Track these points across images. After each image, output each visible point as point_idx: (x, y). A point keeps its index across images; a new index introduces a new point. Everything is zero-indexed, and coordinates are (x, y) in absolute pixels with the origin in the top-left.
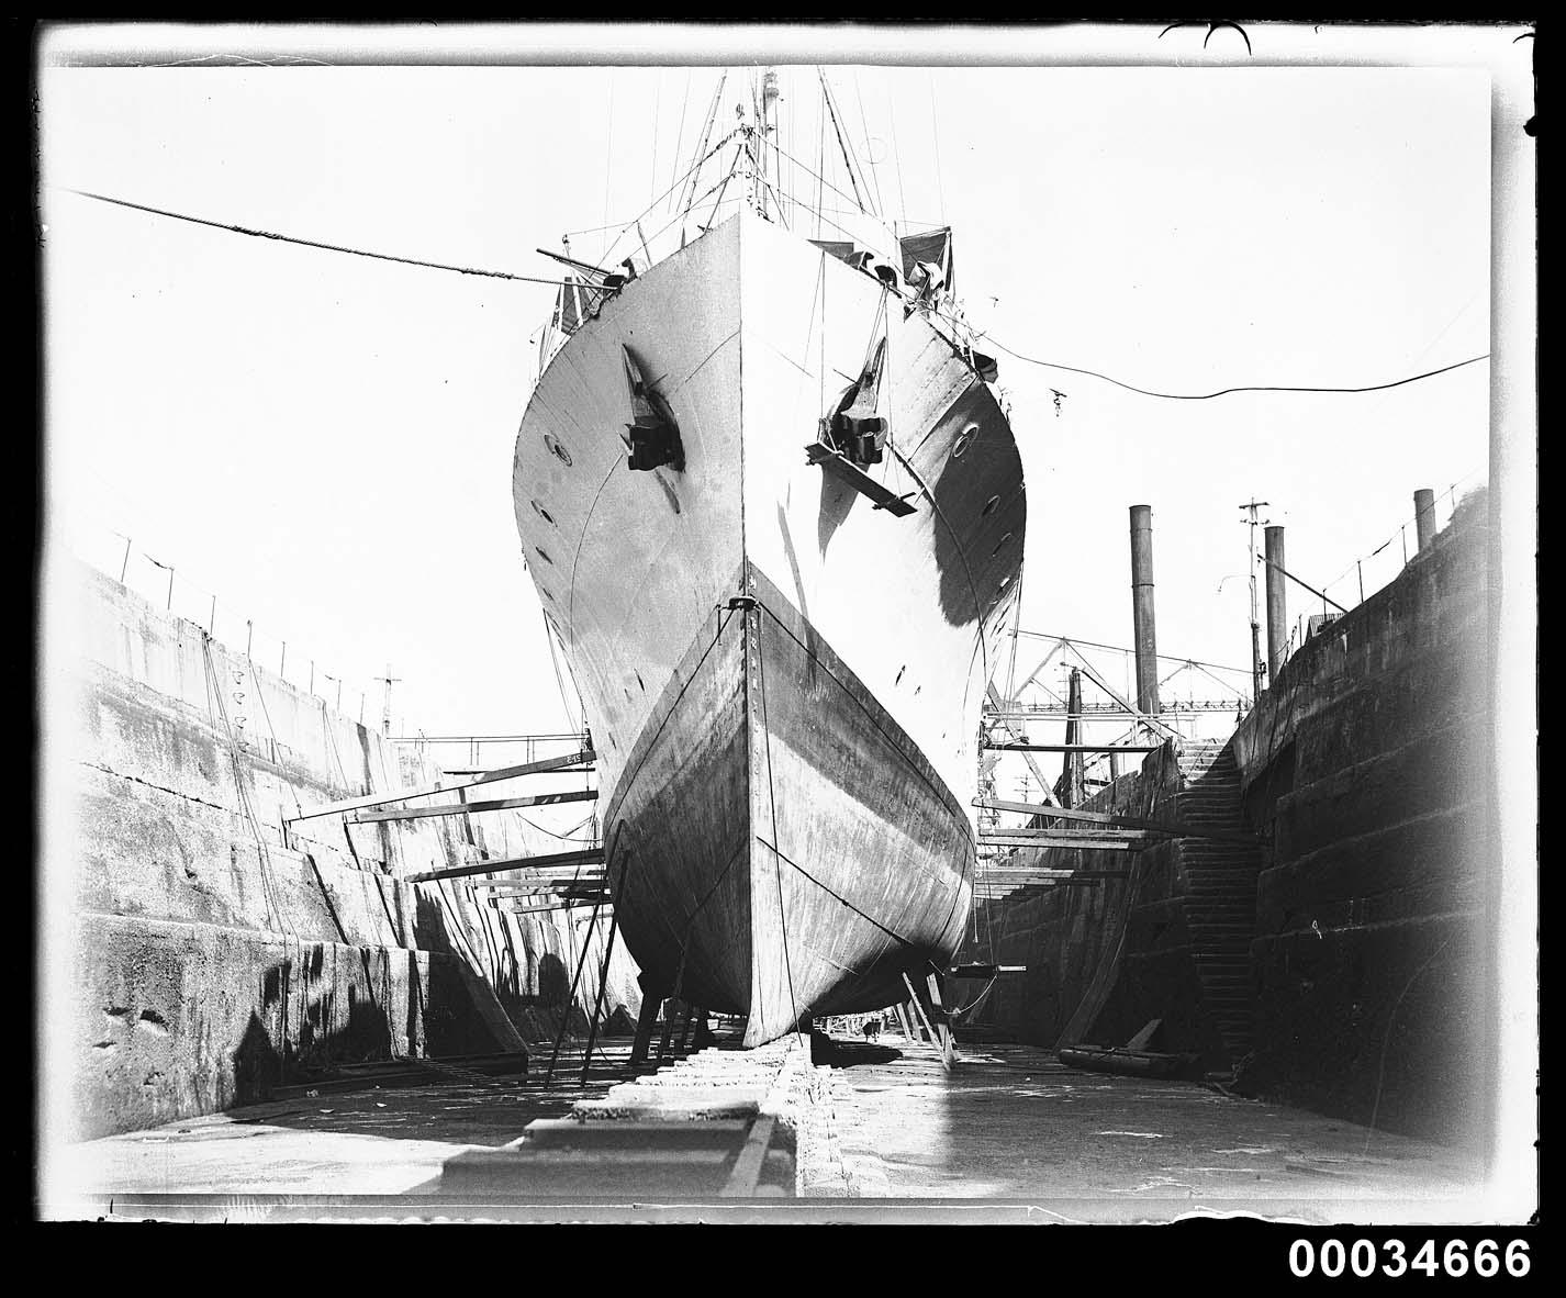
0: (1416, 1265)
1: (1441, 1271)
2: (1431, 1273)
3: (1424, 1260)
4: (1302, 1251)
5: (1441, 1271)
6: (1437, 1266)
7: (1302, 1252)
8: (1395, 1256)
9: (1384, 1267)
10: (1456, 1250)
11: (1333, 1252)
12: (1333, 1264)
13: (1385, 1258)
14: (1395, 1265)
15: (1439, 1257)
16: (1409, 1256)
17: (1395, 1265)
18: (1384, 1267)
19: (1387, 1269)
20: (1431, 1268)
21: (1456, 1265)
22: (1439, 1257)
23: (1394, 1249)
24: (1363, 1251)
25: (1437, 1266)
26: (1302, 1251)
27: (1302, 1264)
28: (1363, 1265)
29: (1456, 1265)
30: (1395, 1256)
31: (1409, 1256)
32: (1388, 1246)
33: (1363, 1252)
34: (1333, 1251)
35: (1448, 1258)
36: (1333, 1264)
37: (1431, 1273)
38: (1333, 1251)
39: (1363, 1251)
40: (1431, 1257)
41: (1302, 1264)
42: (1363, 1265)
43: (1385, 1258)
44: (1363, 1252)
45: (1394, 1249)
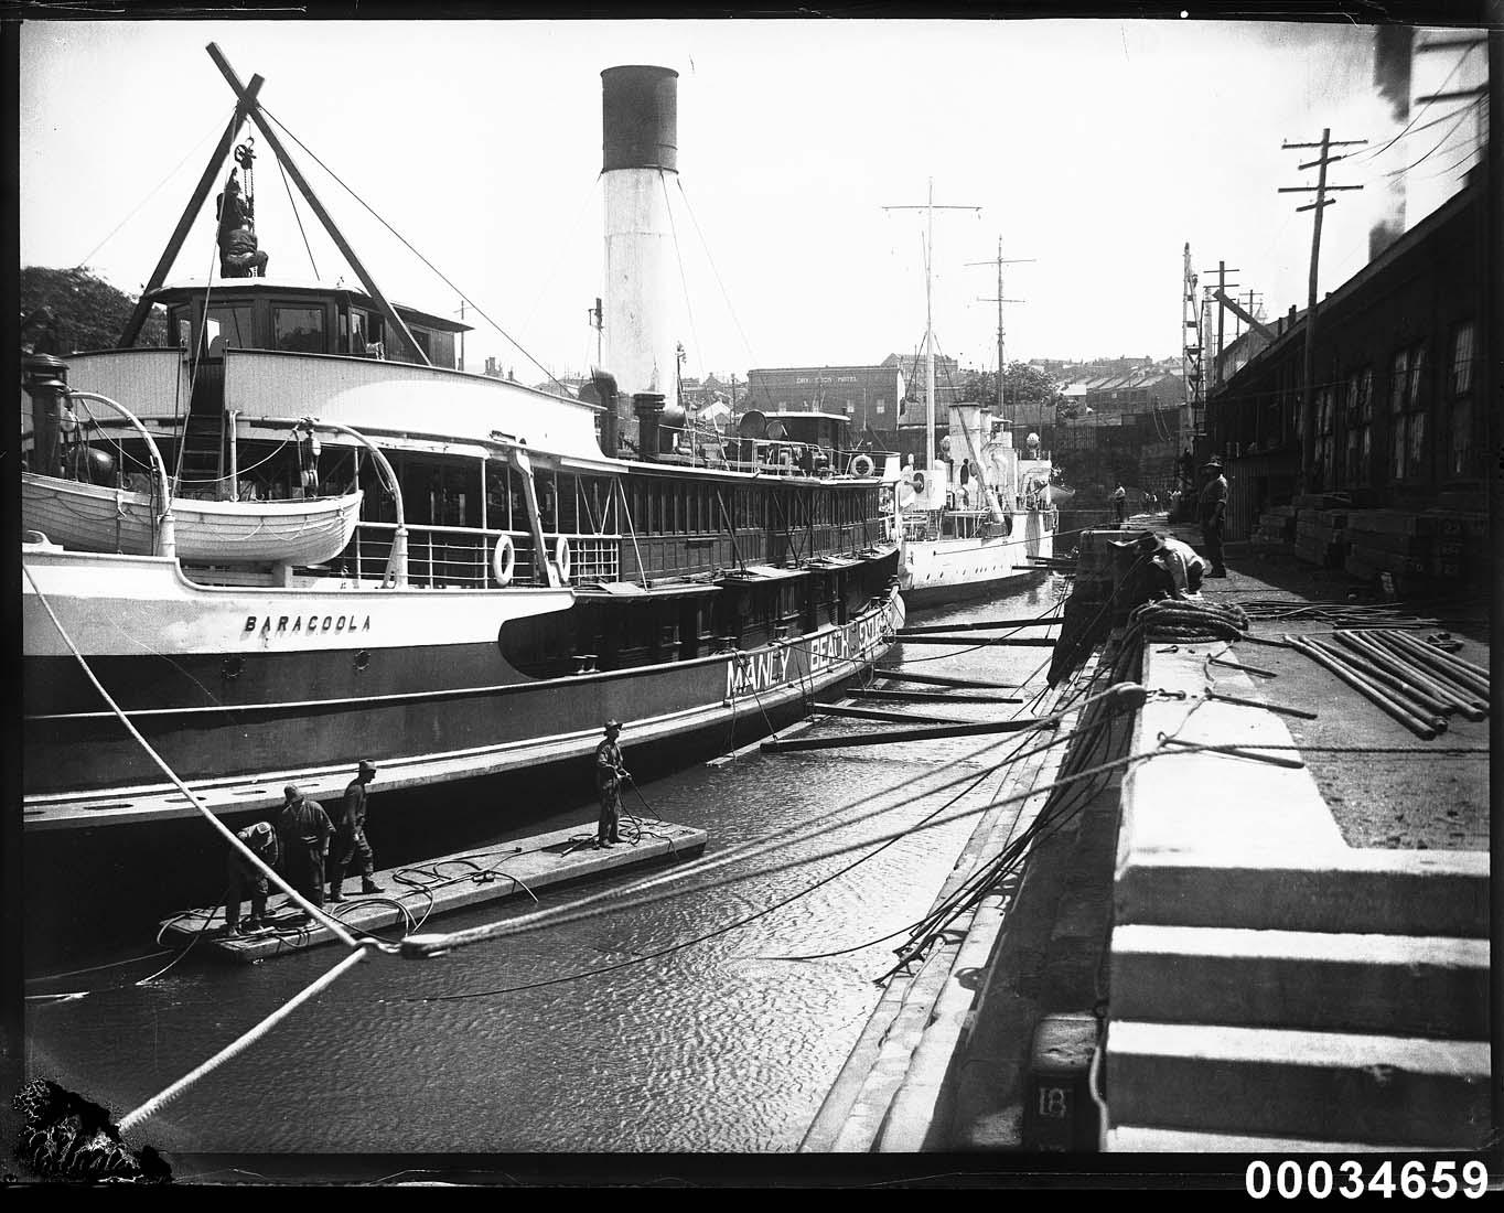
0: (1373, 1186)
1: (1398, 1193)
2: (1388, 1195)
3: (1381, 1181)
4: (1258, 1172)
5: (1398, 1193)
6: (1394, 1187)
7: (1258, 1173)
8: (1353, 1178)
9: (1341, 1189)
10: (1413, 1171)
11: (1290, 1173)
12: (1290, 1185)
13: (1342, 1179)
14: (1352, 1187)
15: (1396, 1179)
16: (1366, 1178)
17: (1352, 1187)
18: (1341, 1189)
19: (1344, 1191)
20: (1388, 1189)
21: (1413, 1186)
22: (1396, 1179)
23: (1351, 1171)
24: (1320, 1172)
25: (1394, 1187)
26: (1258, 1172)
27: (1258, 1186)
28: (1320, 1185)
29: (1413, 1186)
30: (1353, 1178)
31: (1366, 1178)
32: (1345, 1167)
33: (1320, 1173)
34: (1290, 1172)
35: (1405, 1180)
36: (1290, 1185)
37: (1388, 1195)
38: (1290, 1172)
39: (1320, 1172)
40: (1388, 1178)
41: (1258, 1186)
42: (1320, 1185)
43: (1342, 1179)
44: (1320, 1173)
45: (1351, 1171)
